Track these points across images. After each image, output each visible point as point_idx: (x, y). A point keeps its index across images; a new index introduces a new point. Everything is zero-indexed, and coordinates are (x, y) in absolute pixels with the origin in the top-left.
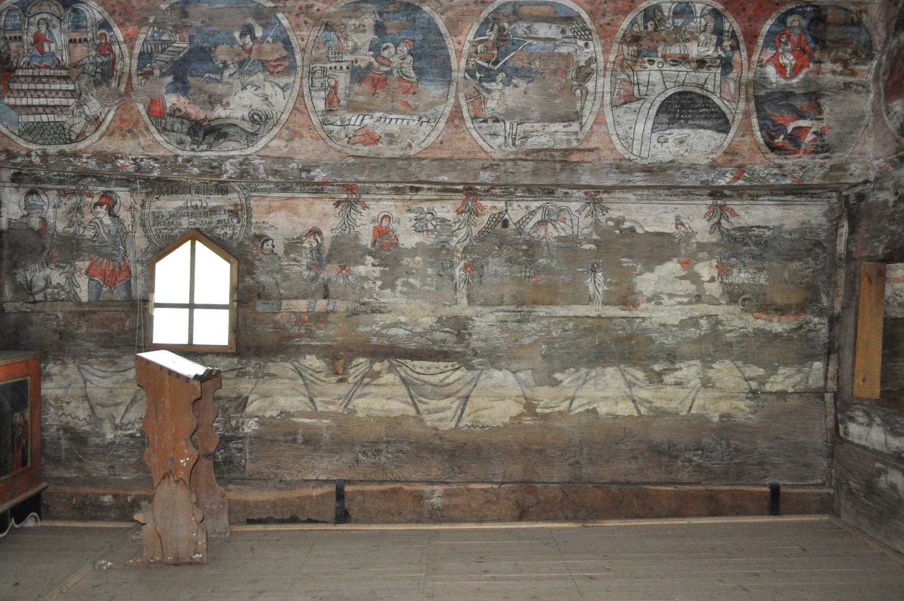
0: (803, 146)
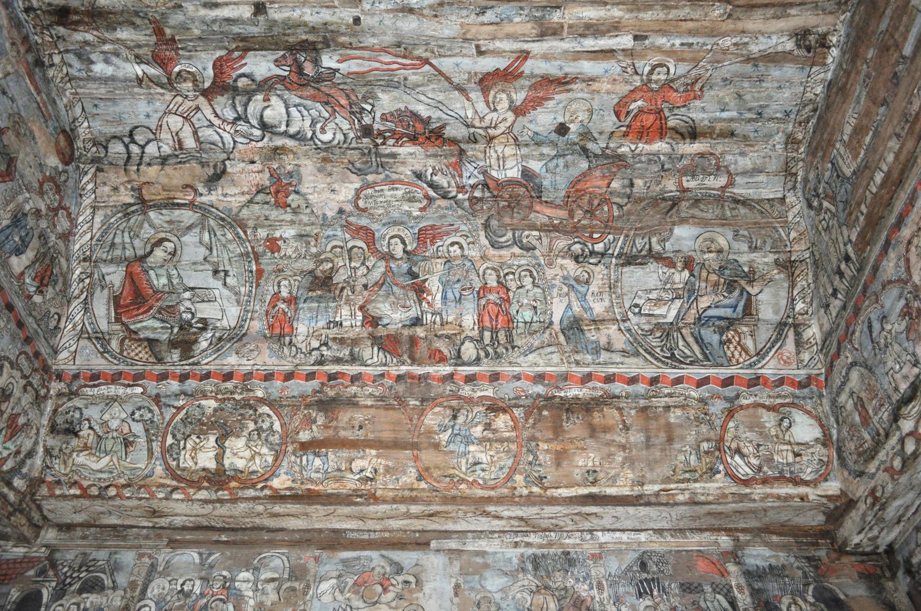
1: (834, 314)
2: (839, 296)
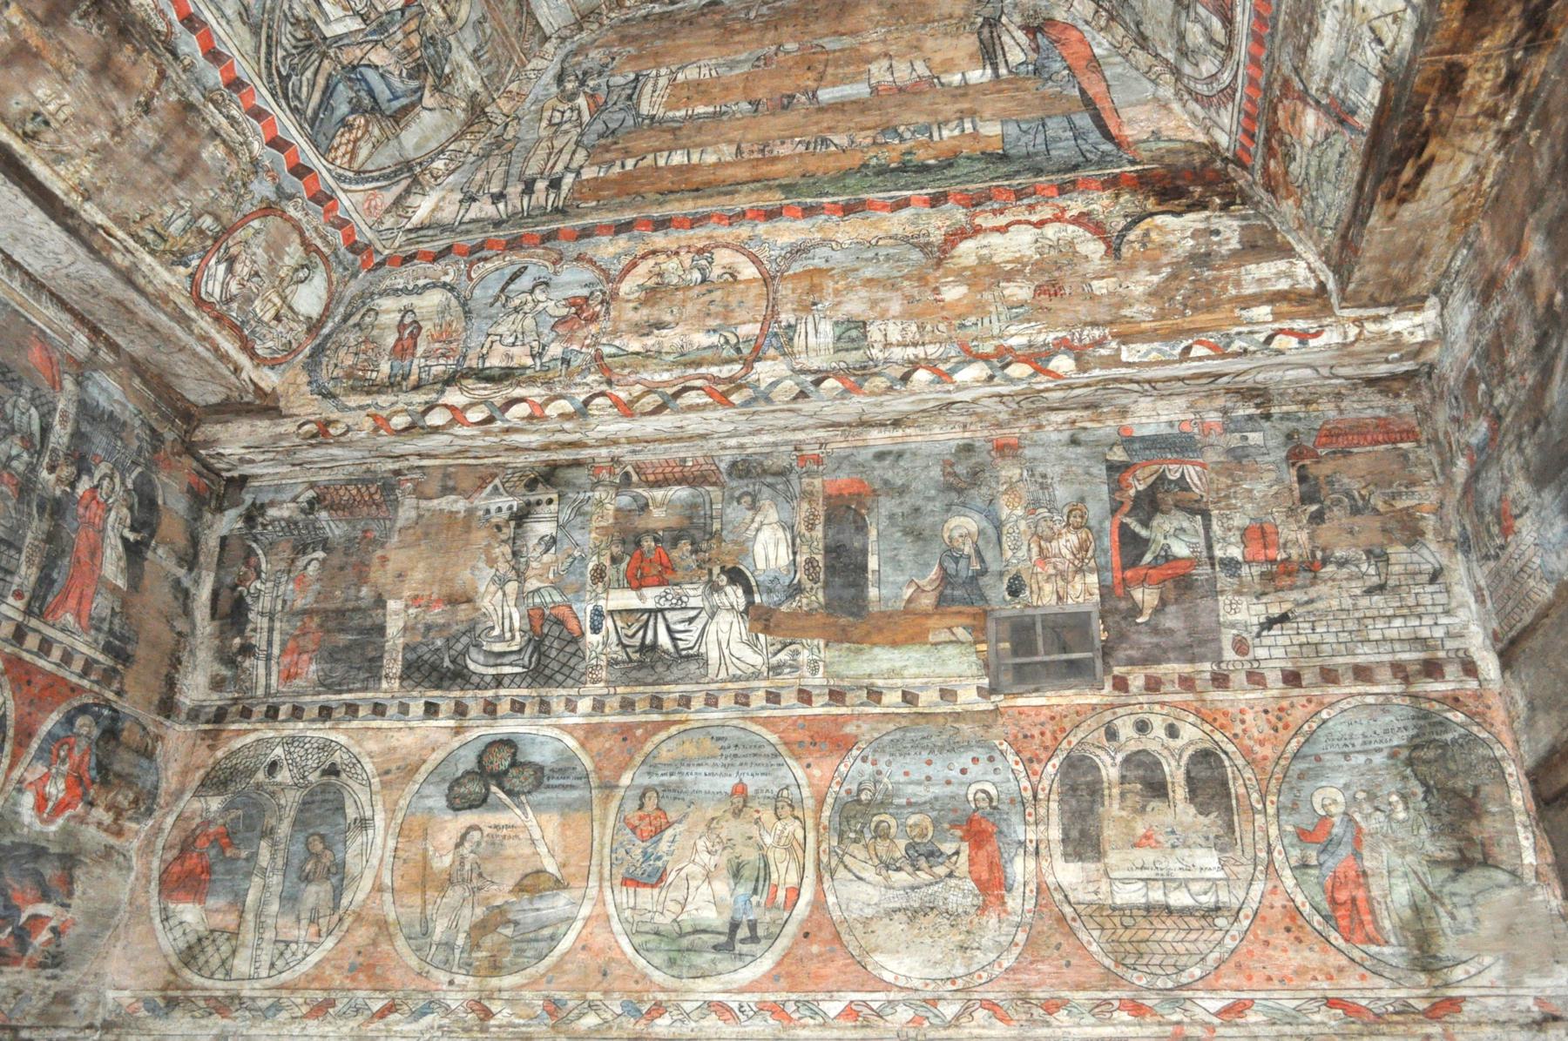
0: (30, 952)
1: (472, 215)
2: (501, 206)
